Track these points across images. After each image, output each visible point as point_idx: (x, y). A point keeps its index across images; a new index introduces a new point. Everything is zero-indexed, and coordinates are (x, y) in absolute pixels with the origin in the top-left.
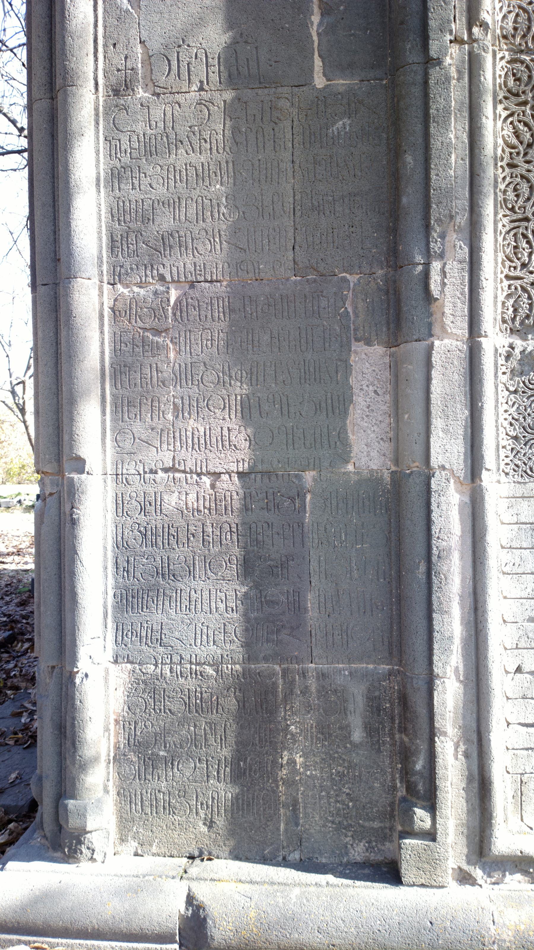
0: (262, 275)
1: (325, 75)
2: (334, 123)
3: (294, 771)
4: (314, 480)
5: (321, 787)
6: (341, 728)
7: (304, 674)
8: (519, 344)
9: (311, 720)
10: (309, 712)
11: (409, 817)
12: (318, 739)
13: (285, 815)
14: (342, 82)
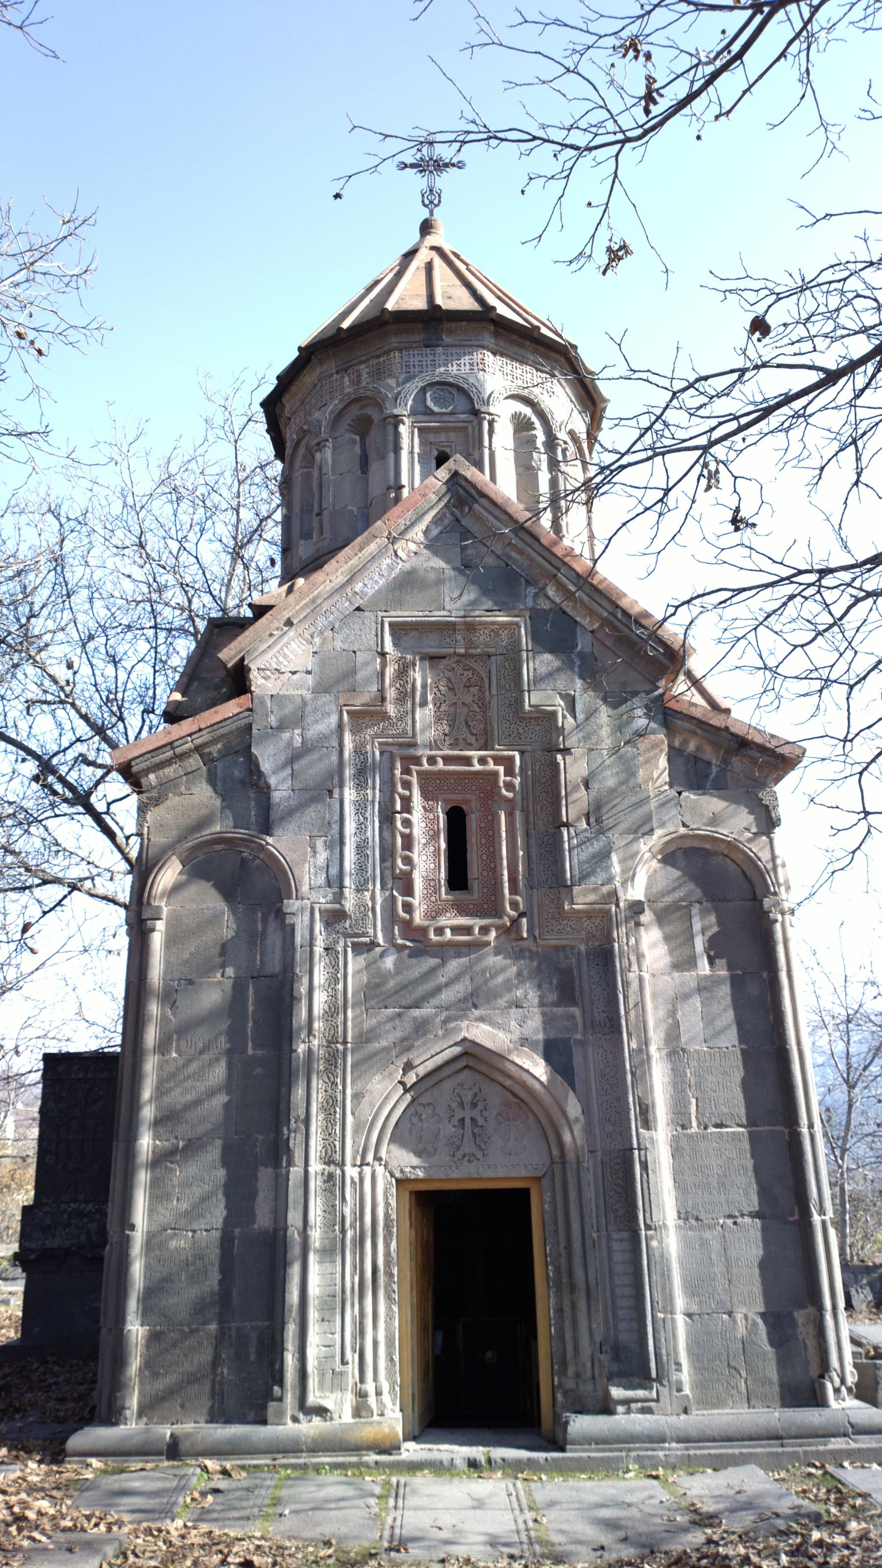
3: (223, 1377)
7: (230, 1329)
8: (326, 1167)
11: (272, 1389)
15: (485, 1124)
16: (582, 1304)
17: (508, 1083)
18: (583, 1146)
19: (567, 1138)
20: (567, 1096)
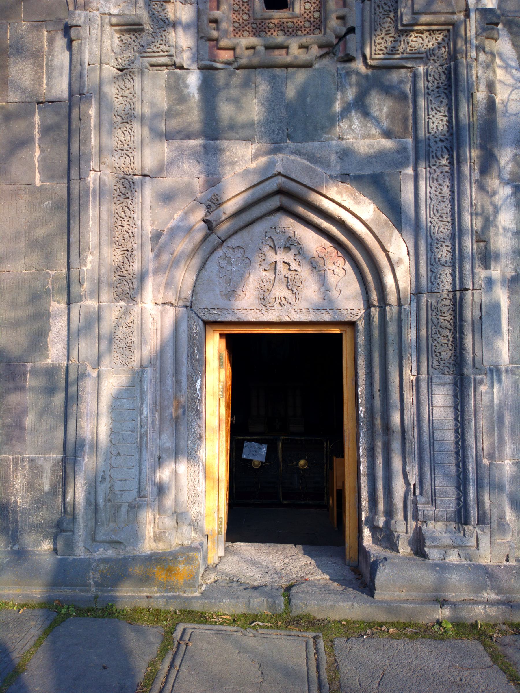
0: (9, 269)
1: (40, 180)
2: (44, 203)
4: (31, 367)
5: (29, 513)
6: (39, 485)
9: (25, 481)
10: (24, 478)
12: (28, 490)
13: (12, 527)
14: (48, 184)
15: (298, 268)
16: (396, 445)
17: (325, 224)
18: (405, 288)
19: (389, 280)
20: (391, 236)
